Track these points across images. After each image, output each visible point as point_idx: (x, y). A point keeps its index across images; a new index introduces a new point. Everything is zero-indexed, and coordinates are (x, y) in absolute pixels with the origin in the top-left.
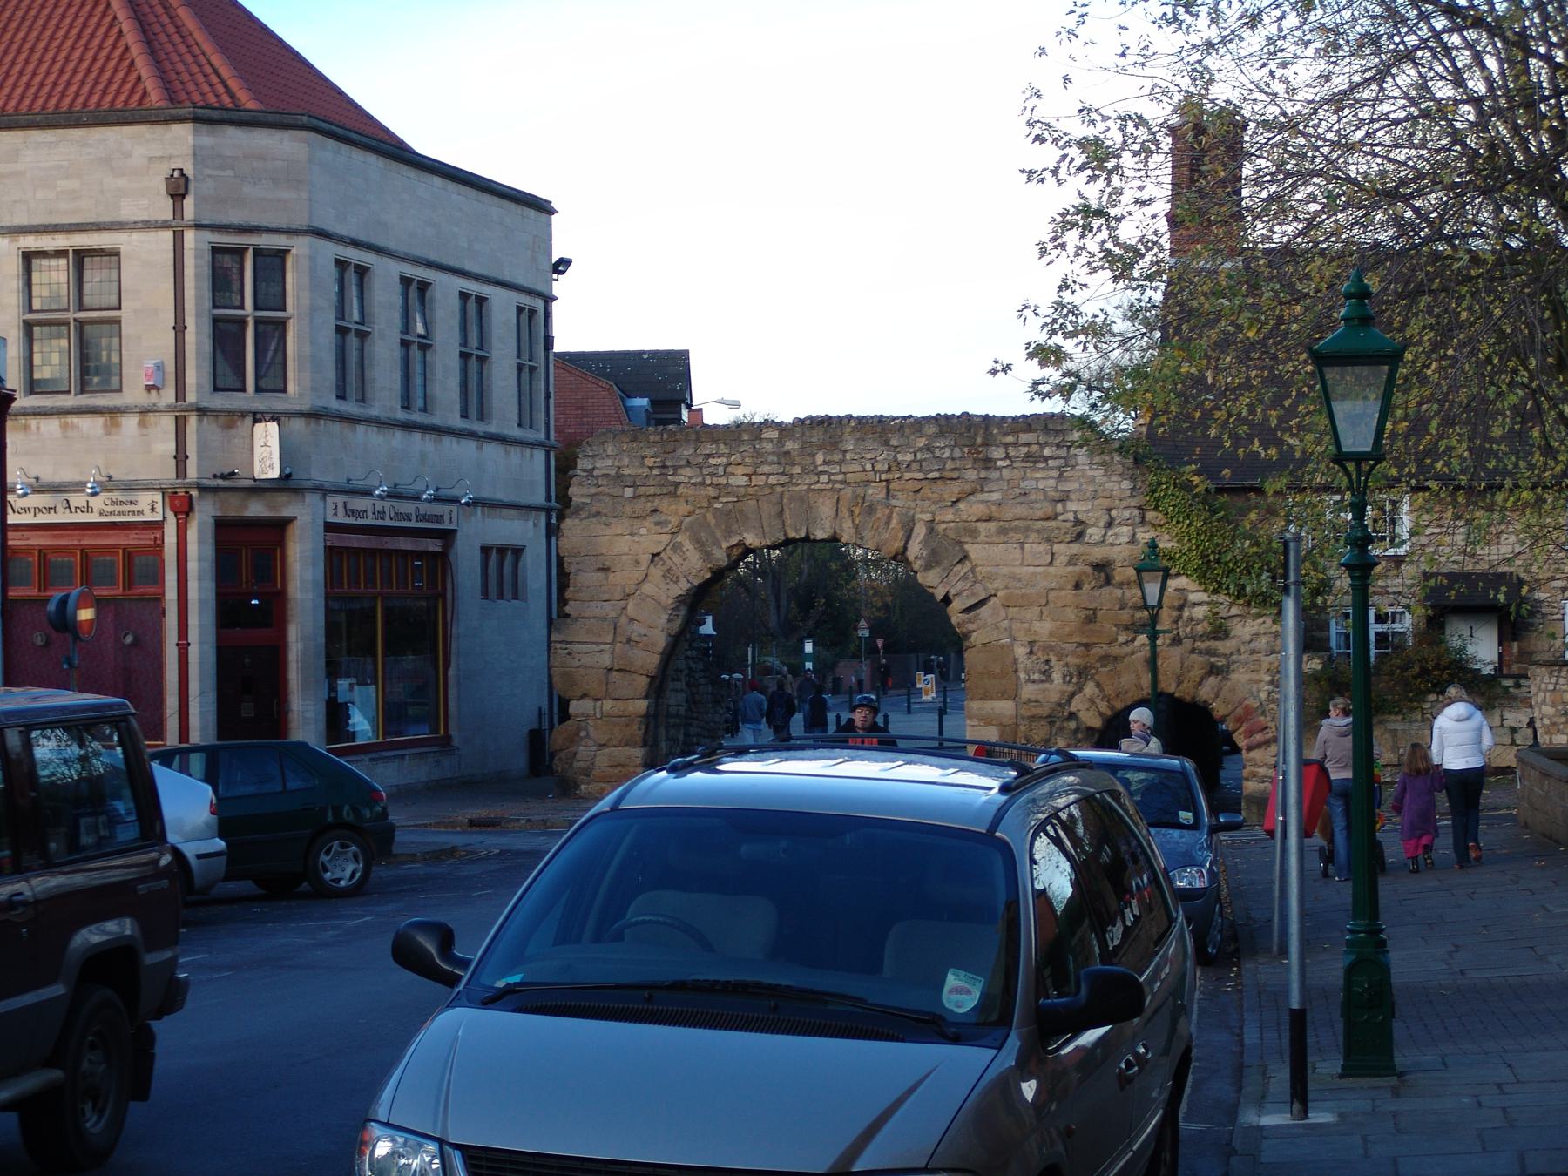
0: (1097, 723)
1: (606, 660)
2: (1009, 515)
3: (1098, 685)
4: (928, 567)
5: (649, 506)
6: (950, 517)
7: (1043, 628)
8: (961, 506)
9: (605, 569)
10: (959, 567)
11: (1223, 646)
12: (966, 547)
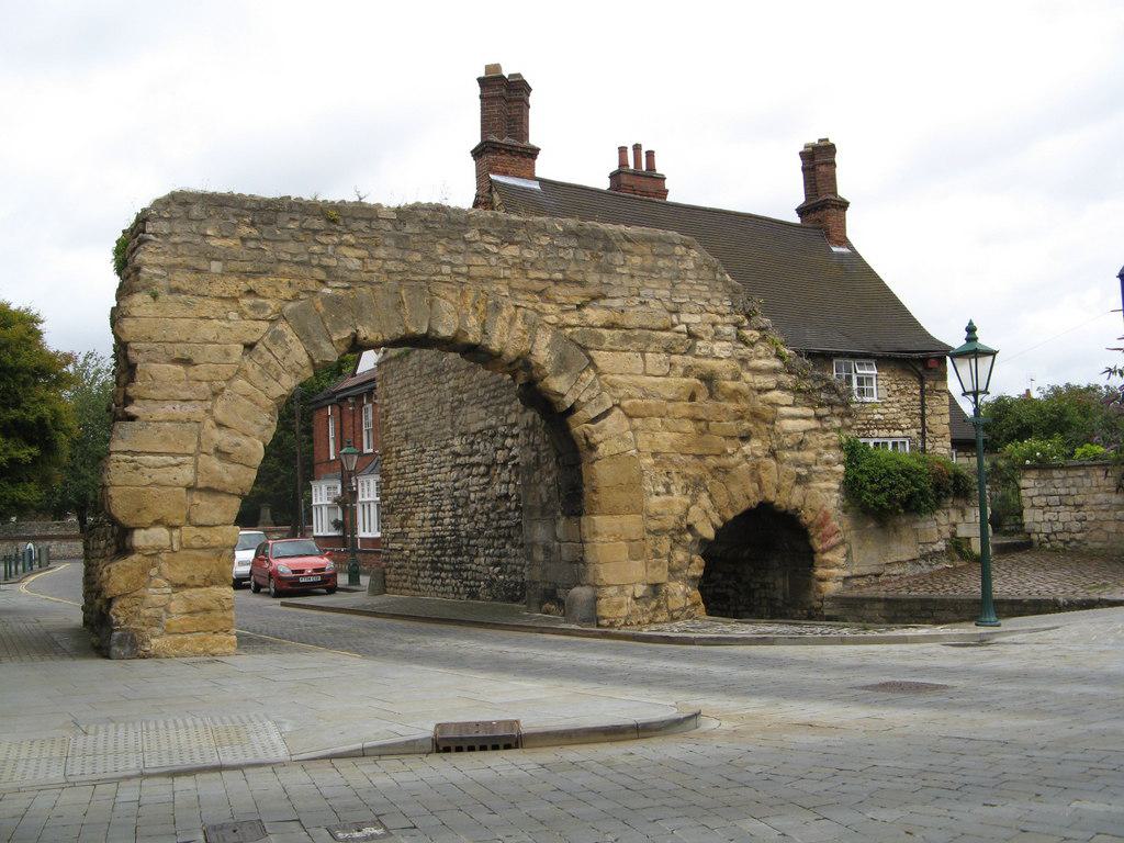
0: (709, 534)
1: (186, 475)
2: (633, 322)
3: (710, 496)
4: (557, 373)
5: (243, 286)
6: (574, 322)
7: (665, 439)
8: (586, 311)
9: (187, 362)
10: (584, 375)
11: (809, 456)
12: (591, 353)
